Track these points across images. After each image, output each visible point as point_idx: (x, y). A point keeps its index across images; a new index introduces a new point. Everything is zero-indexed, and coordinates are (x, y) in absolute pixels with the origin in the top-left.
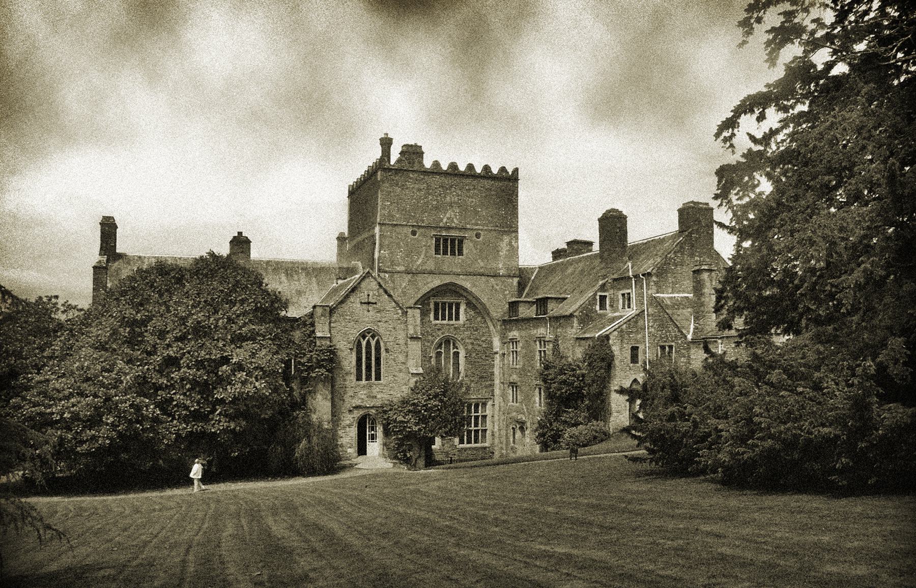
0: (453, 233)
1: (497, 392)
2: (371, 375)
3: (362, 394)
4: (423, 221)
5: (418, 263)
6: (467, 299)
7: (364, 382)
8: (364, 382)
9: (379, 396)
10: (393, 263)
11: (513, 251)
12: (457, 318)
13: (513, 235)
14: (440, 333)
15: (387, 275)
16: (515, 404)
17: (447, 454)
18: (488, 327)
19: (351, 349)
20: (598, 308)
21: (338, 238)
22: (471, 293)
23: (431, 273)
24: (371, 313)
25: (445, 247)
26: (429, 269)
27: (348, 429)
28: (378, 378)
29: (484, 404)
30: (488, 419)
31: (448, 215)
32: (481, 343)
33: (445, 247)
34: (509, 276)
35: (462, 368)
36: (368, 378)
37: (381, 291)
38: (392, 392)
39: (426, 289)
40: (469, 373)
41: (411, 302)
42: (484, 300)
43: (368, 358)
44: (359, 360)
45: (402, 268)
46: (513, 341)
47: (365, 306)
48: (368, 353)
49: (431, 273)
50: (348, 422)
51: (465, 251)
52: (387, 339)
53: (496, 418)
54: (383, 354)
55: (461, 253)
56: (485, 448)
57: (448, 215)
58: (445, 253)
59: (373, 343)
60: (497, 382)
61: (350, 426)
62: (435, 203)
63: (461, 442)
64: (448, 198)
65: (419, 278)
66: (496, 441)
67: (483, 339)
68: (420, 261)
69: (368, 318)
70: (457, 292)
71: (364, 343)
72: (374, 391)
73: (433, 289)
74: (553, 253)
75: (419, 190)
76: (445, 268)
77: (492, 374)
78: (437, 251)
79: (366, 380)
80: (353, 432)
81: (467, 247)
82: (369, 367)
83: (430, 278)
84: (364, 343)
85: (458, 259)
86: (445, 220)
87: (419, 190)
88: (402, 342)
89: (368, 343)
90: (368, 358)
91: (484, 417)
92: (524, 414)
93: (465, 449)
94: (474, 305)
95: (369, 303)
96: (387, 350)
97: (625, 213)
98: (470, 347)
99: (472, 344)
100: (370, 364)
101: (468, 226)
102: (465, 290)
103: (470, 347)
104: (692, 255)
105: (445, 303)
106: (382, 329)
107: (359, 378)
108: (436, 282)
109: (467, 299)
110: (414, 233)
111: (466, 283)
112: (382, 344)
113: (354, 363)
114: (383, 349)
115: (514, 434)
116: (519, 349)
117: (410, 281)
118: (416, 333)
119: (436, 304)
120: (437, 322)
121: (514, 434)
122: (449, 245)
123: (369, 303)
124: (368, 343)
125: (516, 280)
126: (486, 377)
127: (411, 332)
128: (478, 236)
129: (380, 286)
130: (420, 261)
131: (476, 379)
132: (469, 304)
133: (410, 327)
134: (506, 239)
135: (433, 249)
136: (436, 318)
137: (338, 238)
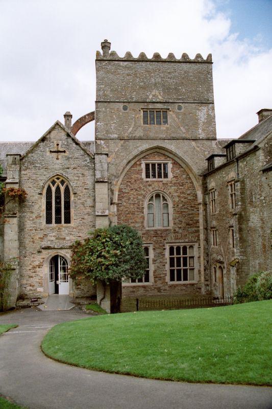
1: (202, 236)
3: (52, 236)
4: (132, 98)
5: (129, 131)
6: (173, 159)
7: (54, 225)
8: (54, 225)
9: (67, 238)
12: (166, 176)
13: (211, 105)
14: (150, 188)
15: (102, 142)
16: (216, 247)
17: (159, 290)
18: (192, 183)
19: (41, 194)
21: (65, 116)
22: (175, 155)
23: (140, 139)
26: (138, 135)
27: (37, 269)
28: (68, 221)
29: (191, 247)
30: (196, 259)
32: (186, 196)
35: (171, 218)
36: (58, 221)
37: (70, 140)
38: (81, 235)
39: (135, 153)
40: (177, 221)
42: (187, 159)
43: (58, 203)
44: (49, 204)
45: (116, 136)
47: (55, 155)
48: (58, 198)
49: (140, 139)
50: (37, 263)
51: (169, 120)
53: (202, 258)
54: (72, 198)
55: (166, 122)
56: (193, 285)
59: (62, 189)
60: (201, 228)
61: (39, 266)
62: (142, 84)
64: (153, 80)
65: (131, 143)
66: (203, 278)
67: (189, 192)
68: (131, 129)
69: (57, 164)
70: (164, 155)
71: (54, 189)
72: (63, 233)
73: (142, 152)
75: (128, 75)
76: (152, 135)
77: (198, 222)
79: (56, 222)
81: (171, 115)
83: (139, 143)
84: (54, 189)
85: (163, 127)
86: (150, 97)
87: (128, 75)
88: (90, 186)
89: (58, 189)
90: (58, 203)
91: (193, 257)
93: (175, 286)
94: (178, 163)
95: (58, 152)
96: (75, 194)
98: (177, 199)
99: (179, 196)
100: (59, 208)
101: (171, 101)
102: (171, 152)
103: (177, 199)
105: (154, 165)
106: (71, 175)
107: (49, 221)
108: (145, 146)
109: (173, 159)
110: (125, 108)
111: (171, 146)
113: (44, 207)
115: (215, 272)
116: (216, 197)
117: (122, 146)
118: (103, 177)
119: (147, 165)
120: (148, 179)
121: (215, 272)
123: (58, 152)
127: (98, 175)
128: (180, 108)
130: (131, 129)
131: (183, 225)
132: (175, 163)
136: (148, 176)
137: (65, 116)
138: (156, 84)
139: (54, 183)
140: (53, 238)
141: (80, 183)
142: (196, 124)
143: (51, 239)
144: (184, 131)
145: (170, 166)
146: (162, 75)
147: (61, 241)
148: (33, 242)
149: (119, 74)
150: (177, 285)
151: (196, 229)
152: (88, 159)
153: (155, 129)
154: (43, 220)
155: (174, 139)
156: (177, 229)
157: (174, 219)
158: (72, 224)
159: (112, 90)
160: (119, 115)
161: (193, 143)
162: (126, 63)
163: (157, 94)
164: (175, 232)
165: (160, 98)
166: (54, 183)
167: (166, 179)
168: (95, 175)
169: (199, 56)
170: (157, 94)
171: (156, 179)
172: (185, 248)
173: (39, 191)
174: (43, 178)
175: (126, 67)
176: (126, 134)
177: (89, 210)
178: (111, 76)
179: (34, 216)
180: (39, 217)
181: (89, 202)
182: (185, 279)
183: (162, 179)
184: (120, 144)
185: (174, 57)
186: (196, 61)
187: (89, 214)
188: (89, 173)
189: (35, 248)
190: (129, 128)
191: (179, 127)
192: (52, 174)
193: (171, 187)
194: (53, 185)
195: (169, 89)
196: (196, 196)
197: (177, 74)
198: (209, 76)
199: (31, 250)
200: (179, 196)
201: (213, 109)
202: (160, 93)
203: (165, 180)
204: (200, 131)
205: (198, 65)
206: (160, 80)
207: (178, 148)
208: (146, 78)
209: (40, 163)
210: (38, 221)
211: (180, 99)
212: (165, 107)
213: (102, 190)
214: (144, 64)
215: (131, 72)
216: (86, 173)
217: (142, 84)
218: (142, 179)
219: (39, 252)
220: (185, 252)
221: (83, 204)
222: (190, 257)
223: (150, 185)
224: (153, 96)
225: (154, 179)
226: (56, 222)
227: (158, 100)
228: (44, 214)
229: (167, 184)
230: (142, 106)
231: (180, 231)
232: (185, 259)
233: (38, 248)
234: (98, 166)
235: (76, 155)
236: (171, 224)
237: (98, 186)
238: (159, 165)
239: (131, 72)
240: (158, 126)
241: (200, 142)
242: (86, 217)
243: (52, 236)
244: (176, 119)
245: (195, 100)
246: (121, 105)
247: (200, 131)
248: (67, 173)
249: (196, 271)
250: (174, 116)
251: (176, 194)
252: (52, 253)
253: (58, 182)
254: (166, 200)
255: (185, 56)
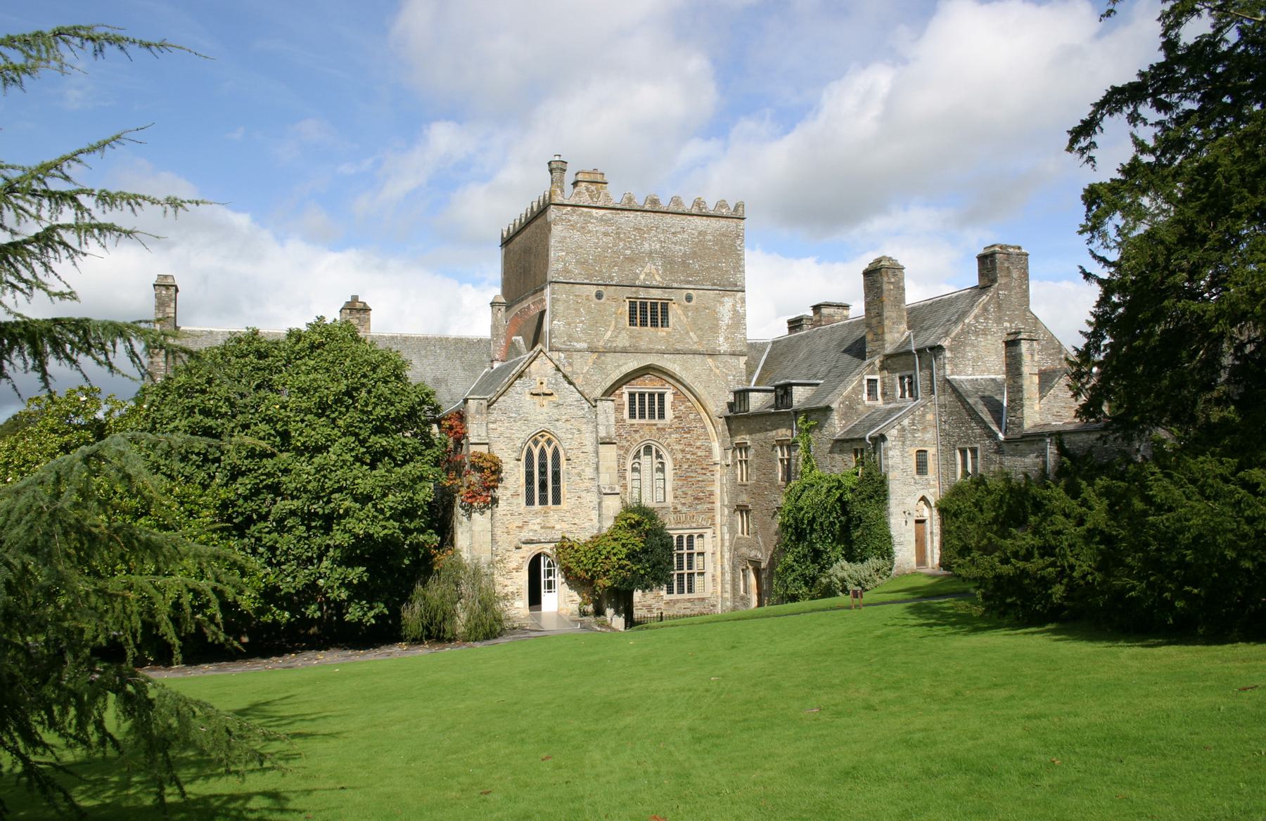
0: (656, 294)
1: (718, 519)
2: (546, 497)
3: (535, 524)
4: (611, 278)
8: (537, 506)
9: (558, 527)
10: (571, 338)
11: (738, 320)
12: (662, 416)
14: (637, 436)
15: (562, 355)
18: (704, 427)
20: (865, 396)
23: (624, 351)
24: (545, 409)
25: (643, 311)
27: (514, 573)
28: (557, 500)
29: (701, 536)
30: (708, 556)
31: (647, 270)
32: (695, 450)
33: (643, 311)
34: (733, 354)
35: (669, 488)
36: (543, 501)
38: (576, 521)
39: (616, 376)
40: (679, 492)
41: (598, 392)
43: (543, 473)
45: (585, 345)
46: (742, 447)
48: (543, 466)
49: (624, 351)
50: (514, 565)
51: (671, 323)
52: (566, 446)
55: (665, 323)
56: (703, 599)
57: (647, 270)
58: (643, 323)
59: (549, 452)
60: (718, 505)
61: (517, 570)
62: (628, 252)
63: (670, 591)
64: (646, 246)
65: (609, 358)
67: (698, 444)
68: (609, 333)
69: (540, 414)
71: (536, 452)
74: (790, 322)
75: (606, 234)
76: (643, 345)
77: (711, 494)
78: (632, 322)
79: (541, 503)
80: (523, 578)
81: (675, 311)
82: (543, 486)
84: (536, 452)
85: (662, 332)
86: (642, 277)
87: (606, 234)
88: (590, 448)
89: (543, 453)
90: (543, 473)
92: (760, 550)
97: (901, 263)
98: (680, 456)
99: (683, 451)
100: (545, 483)
101: (675, 285)
103: (680, 456)
104: (999, 320)
105: (642, 395)
106: (561, 430)
107: (530, 501)
108: (632, 364)
110: (599, 296)
112: (562, 453)
113: (523, 480)
114: (563, 459)
115: (745, 576)
116: (750, 458)
119: (632, 395)
120: (633, 421)
122: (648, 313)
124: (543, 453)
125: (743, 359)
126: (703, 498)
127: (602, 434)
128: (689, 298)
129: (558, 369)
130: (609, 333)
131: (690, 499)
133: (601, 428)
134: (728, 302)
135: (627, 319)
136: (632, 416)
138: (651, 253)
139: (536, 443)
140: (537, 527)
141: (575, 444)
142: (715, 328)
143: (534, 528)
144: (696, 339)
145: (669, 398)
146: (662, 237)
147: (548, 531)
148: (508, 533)
149: (589, 232)
150: (678, 601)
151: (709, 506)
152: (586, 405)
153: (649, 335)
154: (522, 500)
155: (678, 352)
156: (679, 507)
157: (675, 489)
158: (564, 505)
159: (578, 262)
160: (590, 307)
161: (709, 360)
162: (602, 212)
163: (654, 271)
164: (676, 510)
165: (658, 280)
166: (536, 443)
167: (662, 422)
168: (597, 432)
169: (722, 204)
170: (654, 271)
171: (646, 421)
172: (690, 538)
173: (515, 455)
174: (521, 434)
175: (601, 220)
176: (602, 343)
177: (587, 484)
178: (577, 235)
179: (509, 493)
180: (516, 495)
181: (589, 472)
182: (690, 590)
183: (656, 421)
184: (590, 361)
185: (681, 203)
186: (718, 213)
187: (588, 491)
188: (587, 429)
189: (510, 542)
190: (607, 331)
191: (687, 333)
192: (533, 430)
193: (670, 434)
194: (536, 446)
195: (672, 262)
196: (710, 451)
197: (685, 236)
198: (739, 242)
199: (506, 545)
200: (683, 451)
201: (743, 301)
202: (657, 270)
203: (660, 423)
204: (721, 339)
205: (723, 221)
206: (658, 246)
207: (686, 369)
208: (635, 240)
209: (517, 412)
210: (515, 501)
211: (690, 282)
212: (666, 296)
213: (609, 453)
214: (632, 215)
215: (610, 229)
216: (584, 427)
217: (628, 252)
218: (623, 420)
219: (518, 548)
220: (690, 546)
221: (579, 475)
222: (699, 554)
223: (636, 431)
224: (647, 275)
225: (643, 421)
226: (541, 503)
227: (655, 283)
228: (523, 490)
229: (664, 429)
230: (629, 292)
231: (684, 509)
232: (690, 555)
233: (516, 542)
234: (601, 418)
235: (569, 400)
236: (670, 498)
237: (603, 449)
238: (652, 395)
239: (610, 229)
240: (653, 329)
241: (720, 358)
242: (584, 494)
243: (535, 524)
244: (683, 317)
245: (714, 284)
246: (594, 289)
247: (721, 339)
248: (556, 427)
249: (708, 576)
250: (680, 312)
251: (678, 447)
252: (535, 549)
253: (542, 442)
254: (661, 457)
255: (698, 203)
